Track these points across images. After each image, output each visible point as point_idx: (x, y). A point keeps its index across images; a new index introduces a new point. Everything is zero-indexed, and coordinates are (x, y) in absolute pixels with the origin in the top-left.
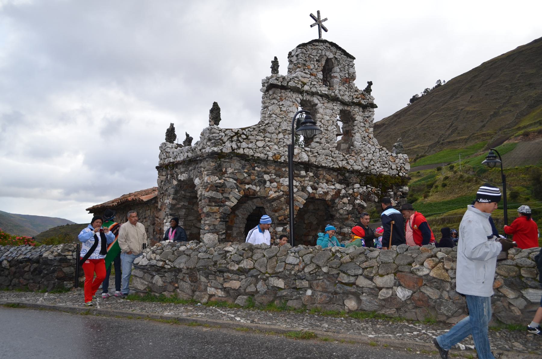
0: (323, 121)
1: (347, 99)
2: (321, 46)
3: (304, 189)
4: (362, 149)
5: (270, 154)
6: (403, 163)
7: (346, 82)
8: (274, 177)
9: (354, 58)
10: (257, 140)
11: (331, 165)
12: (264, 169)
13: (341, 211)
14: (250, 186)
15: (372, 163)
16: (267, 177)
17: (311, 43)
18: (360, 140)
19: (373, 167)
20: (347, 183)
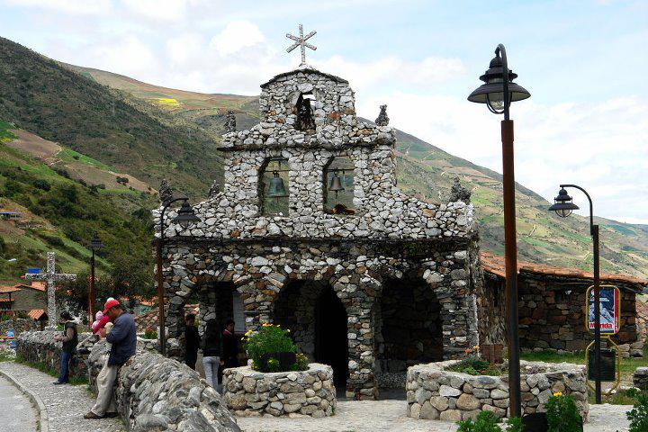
0: (297, 179)
1: (337, 141)
2: (291, 81)
3: (280, 269)
4: (368, 207)
5: (225, 232)
6: (452, 216)
7: (334, 118)
8: (237, 257)
9: (346, 82)
10: (206, 219)
11: (316, 234)
12: (221, 251)
13: (340, 295)
14: (206, 271)
15: (388, 223)
16: (226, 259)
17: (272, 82)
18: (363, 194)
19: (390, 229)
20: (343, 255)
